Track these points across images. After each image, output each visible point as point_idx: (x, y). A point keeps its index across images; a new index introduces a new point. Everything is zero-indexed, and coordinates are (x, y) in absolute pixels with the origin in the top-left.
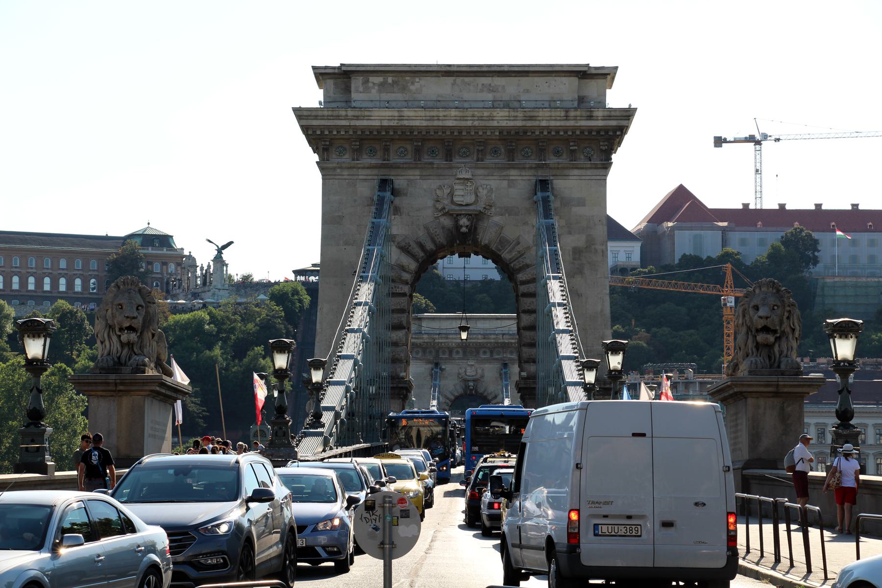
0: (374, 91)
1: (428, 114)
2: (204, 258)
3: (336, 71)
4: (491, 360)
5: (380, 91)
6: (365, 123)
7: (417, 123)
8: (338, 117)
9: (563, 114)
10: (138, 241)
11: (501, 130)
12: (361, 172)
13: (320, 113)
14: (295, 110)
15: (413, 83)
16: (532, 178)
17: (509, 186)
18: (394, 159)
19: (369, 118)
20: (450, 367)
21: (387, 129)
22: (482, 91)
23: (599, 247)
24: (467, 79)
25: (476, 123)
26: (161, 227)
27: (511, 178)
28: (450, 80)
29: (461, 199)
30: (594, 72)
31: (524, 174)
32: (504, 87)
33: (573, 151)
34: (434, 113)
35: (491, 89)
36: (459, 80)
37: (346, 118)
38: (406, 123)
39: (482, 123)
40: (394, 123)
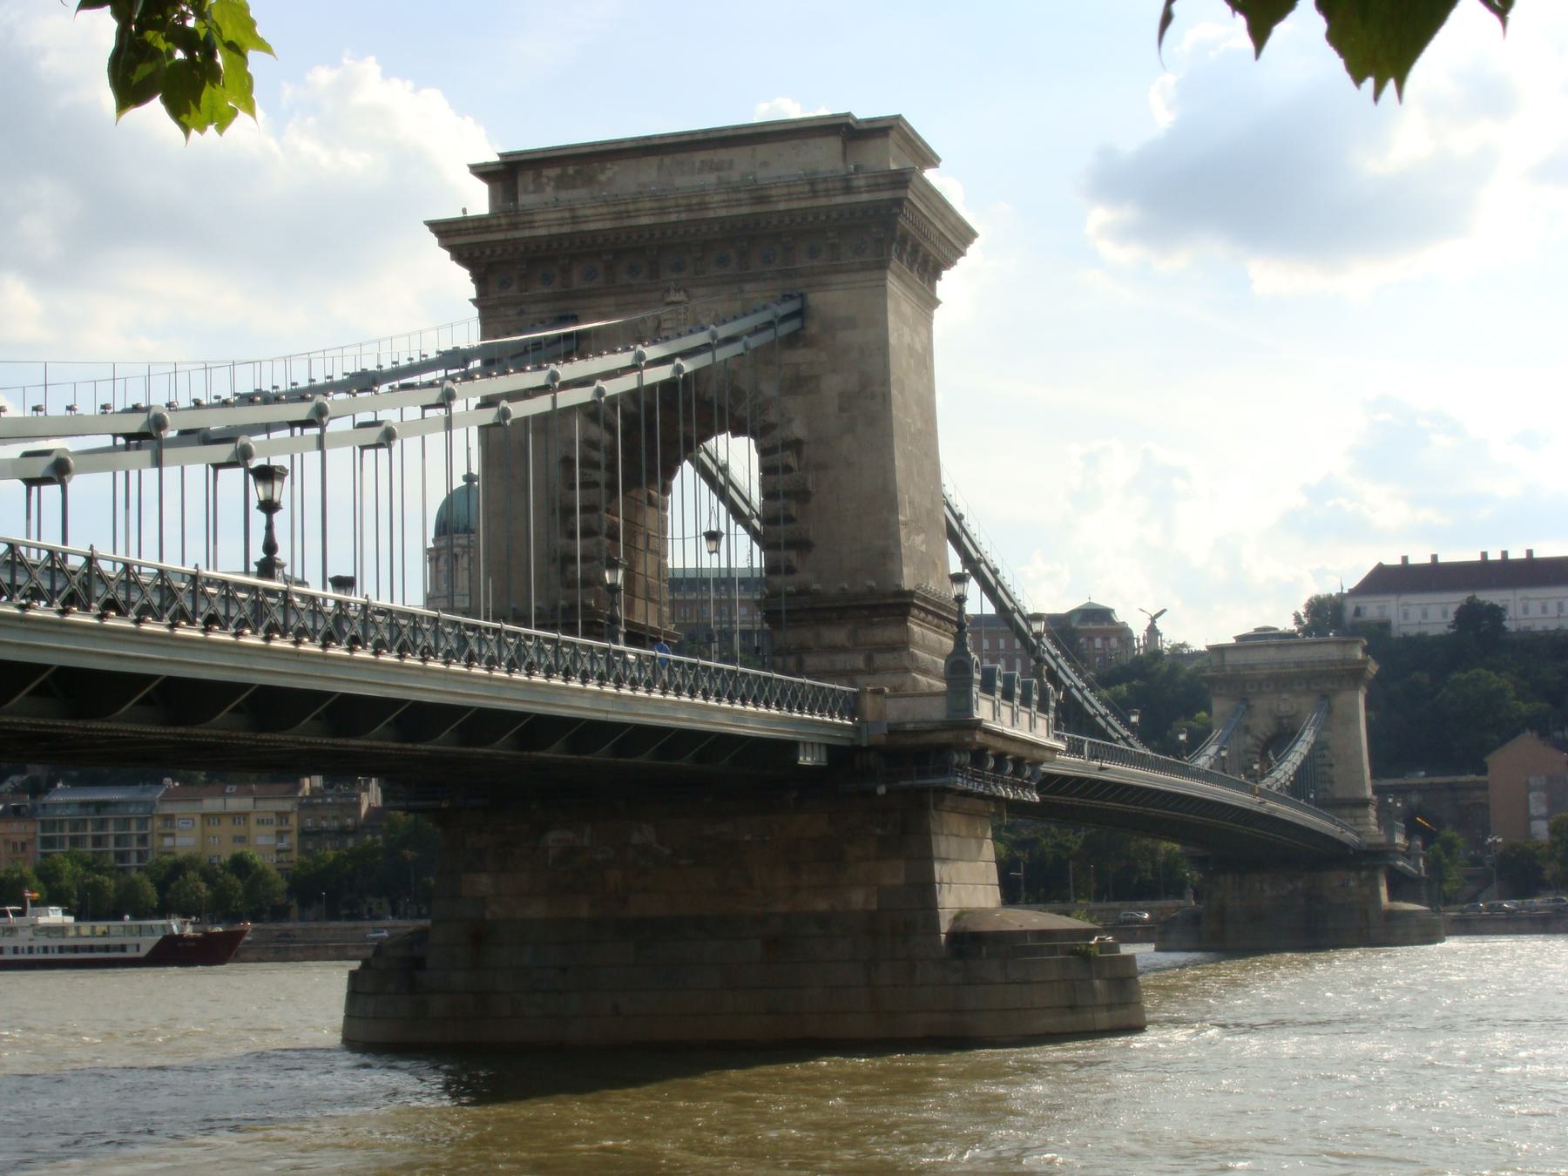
0: (549, 189)
1: (612, 209)
2: (1139, 630)
5: (557, 188)
6: (527, 233)
9: (807, 188)
10: (1077, 618)
15: (602, 171)
19: (530, 225)
21: (560, 237)
22: (701, 171)
24: (680, 157)
25: (684, 217)
26: (1102, 601)
28: (654, 160)
30: (866, 126)
32: (731, 163)
34: (622, 208)
35: (715, 167)
36: (667, 160)
40: (566, 229)
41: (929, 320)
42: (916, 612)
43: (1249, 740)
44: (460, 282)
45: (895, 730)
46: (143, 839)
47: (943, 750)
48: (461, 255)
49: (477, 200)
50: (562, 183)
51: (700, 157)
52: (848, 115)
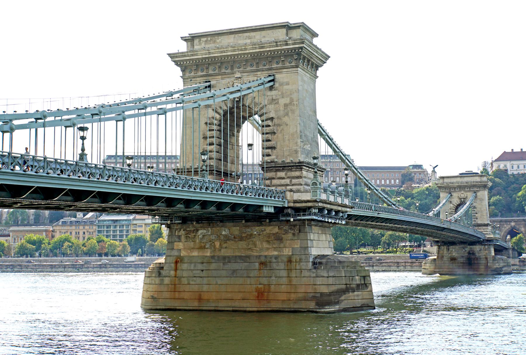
0: (203, 44)
1: (220, 50)
2: (430, 170)
4: (470, 191)
5: (205, 44)
6: (196, 57)
9: (275, 44)
13: (178, 55)
14: (169, 54)
18: (211, 72)
19: (197, 55)
20: (455, 195)
22: (246, 39)
23: (295, 103)
24: (240, 35)
25: (240, 52)
28: (233, 36)
35: (250, 38)
36: (236, 35)
38: (212, 55)
39: (242, 52)
41: (315, 82)
42: (305, 168)
43: (452, 205)
44: (178, 71)
45: (295, 202)
46: (127, 231)
47: (310, 208)
48: (177, 63)
49: (183, 47)
52: (288, 22)
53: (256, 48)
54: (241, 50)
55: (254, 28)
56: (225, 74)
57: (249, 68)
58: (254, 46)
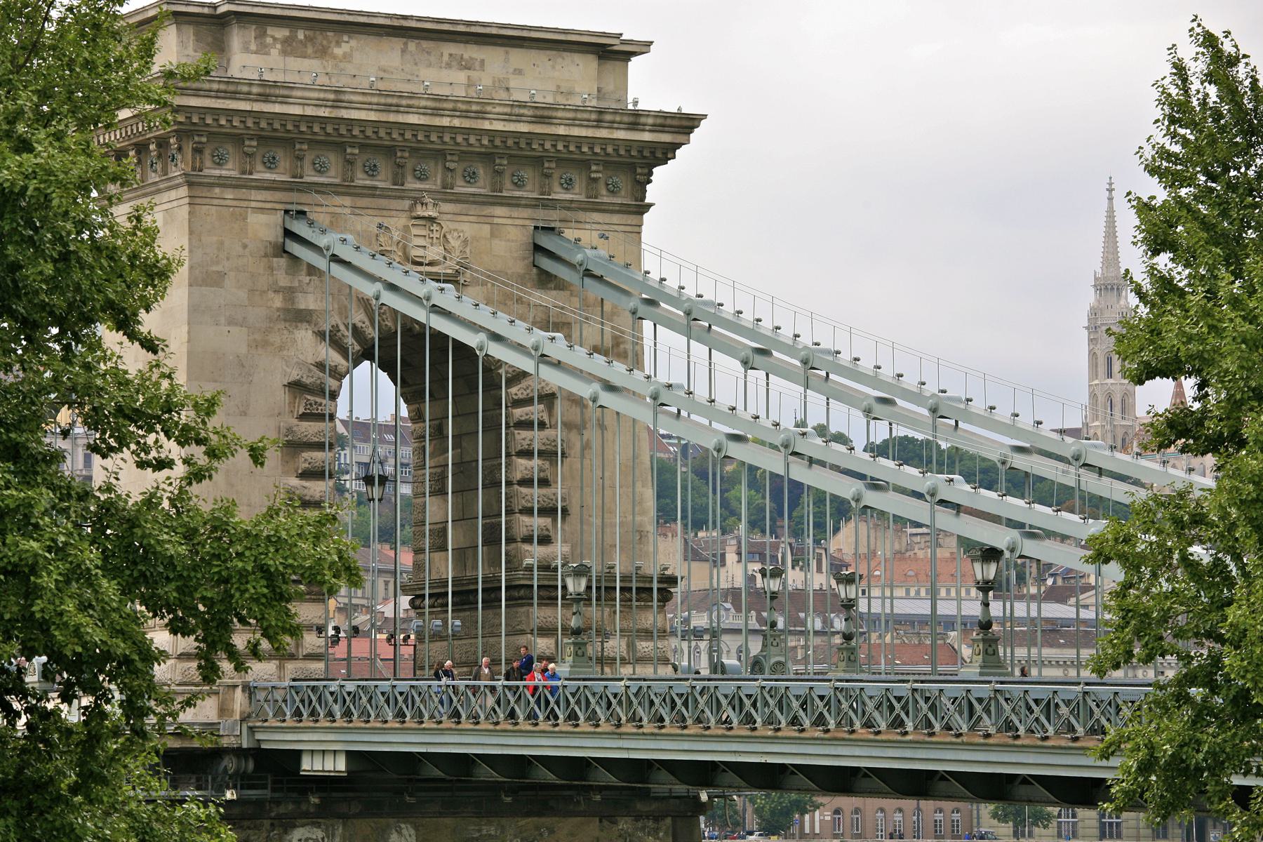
0: (275, 52)
1: (383, 100)
3: (206, 11)
5: (284, 53)
6: (277, 108)
7: (362, 115)
8: (234, 95)
9: (594, 116)
11: (492, 134)
12: (255, 195)
15: (338, 44)
16: (527, 223)
17: (493, 235)
19: (284, 100)
22: (449, 66)
24: (425, 44)
25: (457, 122)
27: (496, 220)
28: (398, 43)
29: (420, 252)
31: (515, 214)
32: (482, 61)
33: (595, 180)
34: (394, 101)
36: (412, 45)
37: (247, 97)
39: (467, 123)
50: (289, 47)
51: (449, 49)
53: (518, 118)
54: (465, 114)
55: (494, 31)
56: (372, 192)
57: (462, 188)
58: (517, 111)
